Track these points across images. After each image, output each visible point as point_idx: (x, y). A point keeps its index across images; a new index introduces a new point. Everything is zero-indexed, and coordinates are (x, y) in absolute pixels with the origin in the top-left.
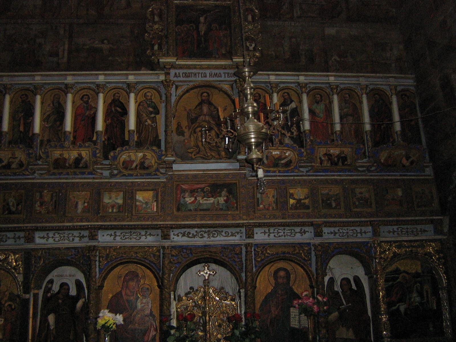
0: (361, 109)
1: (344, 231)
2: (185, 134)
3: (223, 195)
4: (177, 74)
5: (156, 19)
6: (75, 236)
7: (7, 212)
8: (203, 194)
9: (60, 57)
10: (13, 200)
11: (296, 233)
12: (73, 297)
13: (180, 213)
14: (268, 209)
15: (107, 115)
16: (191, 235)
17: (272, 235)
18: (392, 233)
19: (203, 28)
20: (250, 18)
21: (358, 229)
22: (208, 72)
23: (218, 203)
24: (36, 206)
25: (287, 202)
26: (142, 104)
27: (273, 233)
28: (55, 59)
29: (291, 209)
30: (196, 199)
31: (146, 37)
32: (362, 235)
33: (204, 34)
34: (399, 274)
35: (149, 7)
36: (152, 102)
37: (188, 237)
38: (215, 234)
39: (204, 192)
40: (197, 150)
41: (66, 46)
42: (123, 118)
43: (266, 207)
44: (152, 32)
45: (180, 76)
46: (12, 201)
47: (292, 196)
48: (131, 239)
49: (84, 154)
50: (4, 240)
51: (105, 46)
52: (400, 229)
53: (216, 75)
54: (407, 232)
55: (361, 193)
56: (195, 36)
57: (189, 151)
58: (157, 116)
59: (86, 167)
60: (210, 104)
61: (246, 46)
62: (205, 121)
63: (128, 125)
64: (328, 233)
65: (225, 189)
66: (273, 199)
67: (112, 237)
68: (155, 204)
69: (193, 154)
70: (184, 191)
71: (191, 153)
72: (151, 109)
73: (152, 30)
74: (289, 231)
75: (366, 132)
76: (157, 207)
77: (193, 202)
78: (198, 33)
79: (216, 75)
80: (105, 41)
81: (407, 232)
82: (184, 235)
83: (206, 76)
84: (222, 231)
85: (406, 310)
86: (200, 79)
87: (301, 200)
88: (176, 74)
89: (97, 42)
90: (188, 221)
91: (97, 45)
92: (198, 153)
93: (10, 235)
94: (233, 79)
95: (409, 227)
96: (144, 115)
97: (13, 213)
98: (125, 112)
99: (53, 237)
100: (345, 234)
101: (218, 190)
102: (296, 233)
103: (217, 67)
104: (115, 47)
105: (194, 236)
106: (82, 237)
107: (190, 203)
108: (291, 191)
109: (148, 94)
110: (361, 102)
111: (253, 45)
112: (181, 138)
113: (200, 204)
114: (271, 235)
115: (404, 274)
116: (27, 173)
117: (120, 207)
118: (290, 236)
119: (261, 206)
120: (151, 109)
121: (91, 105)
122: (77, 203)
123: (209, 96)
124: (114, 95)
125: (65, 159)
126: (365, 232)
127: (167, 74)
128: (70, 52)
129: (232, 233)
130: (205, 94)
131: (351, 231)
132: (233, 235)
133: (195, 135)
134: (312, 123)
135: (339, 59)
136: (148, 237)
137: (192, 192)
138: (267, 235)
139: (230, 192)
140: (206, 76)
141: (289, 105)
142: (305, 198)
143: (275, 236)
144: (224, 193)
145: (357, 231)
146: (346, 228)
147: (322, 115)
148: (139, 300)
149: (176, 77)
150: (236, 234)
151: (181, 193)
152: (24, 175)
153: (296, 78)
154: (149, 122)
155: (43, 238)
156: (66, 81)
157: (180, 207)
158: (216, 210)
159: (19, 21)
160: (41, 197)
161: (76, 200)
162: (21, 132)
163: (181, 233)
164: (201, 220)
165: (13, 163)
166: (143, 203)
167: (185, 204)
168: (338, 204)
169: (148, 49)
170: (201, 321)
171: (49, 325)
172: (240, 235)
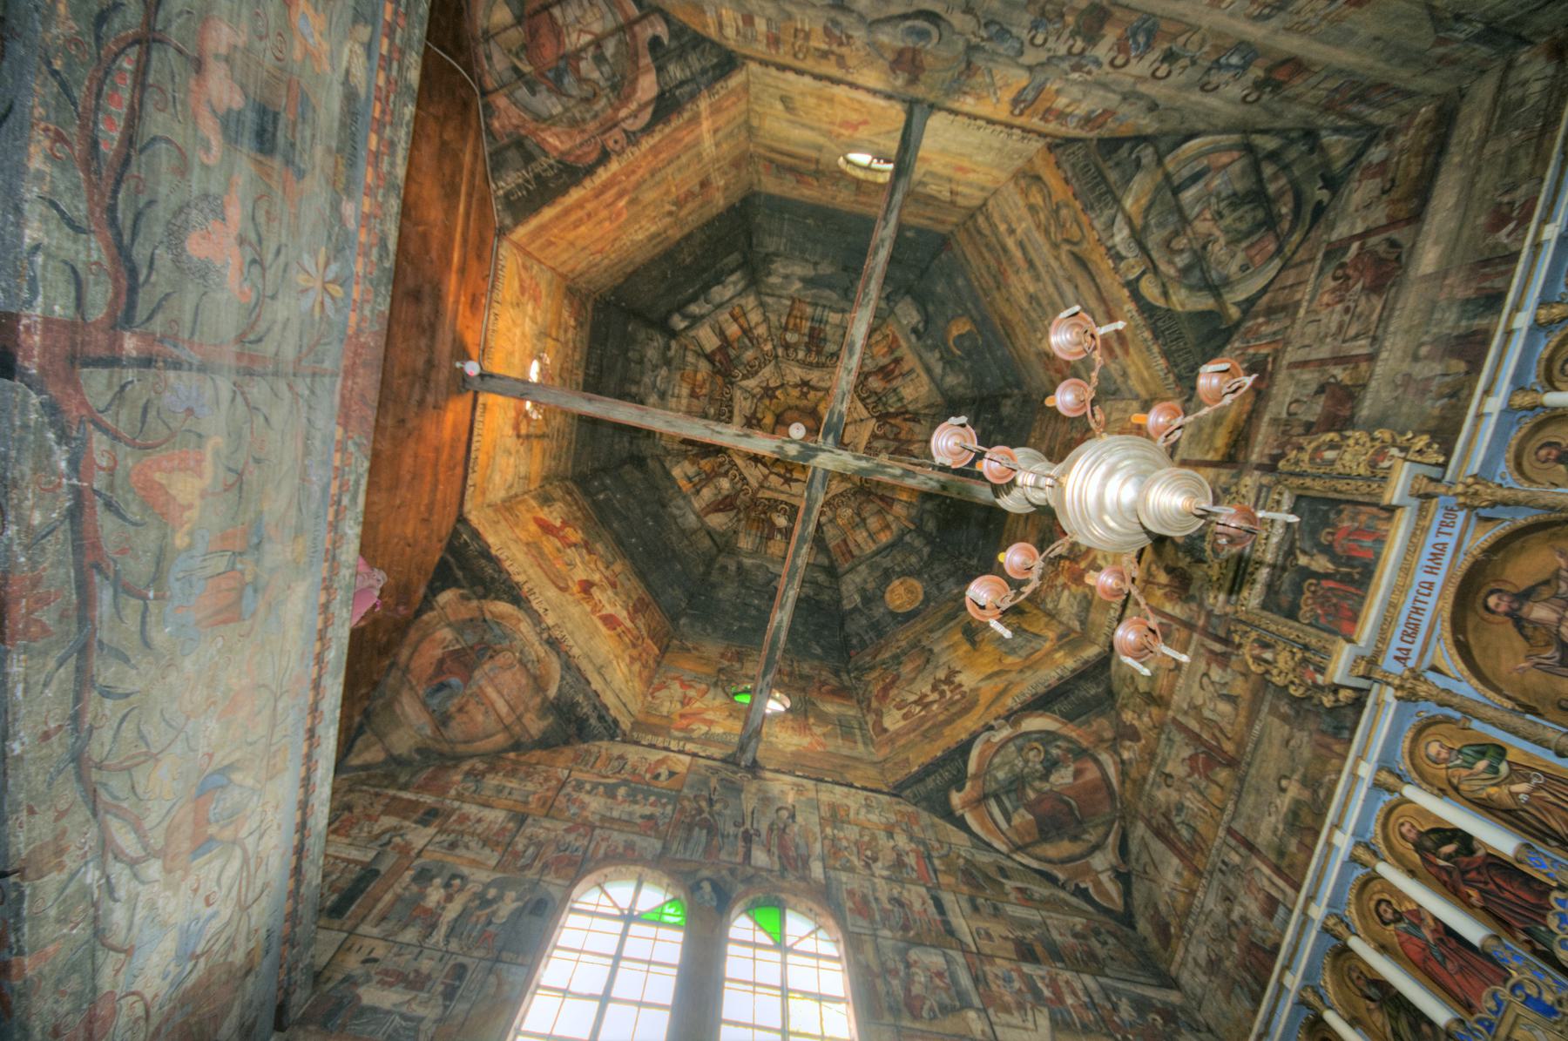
4: (1399, 654)
5: (1268, 655)
15: (1451, 889)
19: (1321, 564)
20: (1329, 455)
22: (1421, 576)
26: (1455, 781)
31: (1297, 694)
33: (1334, 563)
36: (1460, 752)
41: (1266, 870)
42: (1481, 853)
45: (1408, 650)
51: (1294, 790)
56: (1331, 584)
58: (1509, 757)
60: (1527, 595)
78: (1327, 576)
79: (1435, 557)
80: (1284, 783)
83: (1432, 584)
86: (1432, 600)
88: (1397, 658)
89: (1278, 802)
91: (1284, 803)
96: (1493, 790)
98: (1465, 841)
103: (1412, 548)
104: (1302, 770)
109: (1434, 749)
120: (1481, 765)
121: (1409, 912)
123: (1500, 591)
124: (1403, 836)
128: (1277, 870)
135: (1511, 226)
154: (1521, 788)
159: (1190, 922)
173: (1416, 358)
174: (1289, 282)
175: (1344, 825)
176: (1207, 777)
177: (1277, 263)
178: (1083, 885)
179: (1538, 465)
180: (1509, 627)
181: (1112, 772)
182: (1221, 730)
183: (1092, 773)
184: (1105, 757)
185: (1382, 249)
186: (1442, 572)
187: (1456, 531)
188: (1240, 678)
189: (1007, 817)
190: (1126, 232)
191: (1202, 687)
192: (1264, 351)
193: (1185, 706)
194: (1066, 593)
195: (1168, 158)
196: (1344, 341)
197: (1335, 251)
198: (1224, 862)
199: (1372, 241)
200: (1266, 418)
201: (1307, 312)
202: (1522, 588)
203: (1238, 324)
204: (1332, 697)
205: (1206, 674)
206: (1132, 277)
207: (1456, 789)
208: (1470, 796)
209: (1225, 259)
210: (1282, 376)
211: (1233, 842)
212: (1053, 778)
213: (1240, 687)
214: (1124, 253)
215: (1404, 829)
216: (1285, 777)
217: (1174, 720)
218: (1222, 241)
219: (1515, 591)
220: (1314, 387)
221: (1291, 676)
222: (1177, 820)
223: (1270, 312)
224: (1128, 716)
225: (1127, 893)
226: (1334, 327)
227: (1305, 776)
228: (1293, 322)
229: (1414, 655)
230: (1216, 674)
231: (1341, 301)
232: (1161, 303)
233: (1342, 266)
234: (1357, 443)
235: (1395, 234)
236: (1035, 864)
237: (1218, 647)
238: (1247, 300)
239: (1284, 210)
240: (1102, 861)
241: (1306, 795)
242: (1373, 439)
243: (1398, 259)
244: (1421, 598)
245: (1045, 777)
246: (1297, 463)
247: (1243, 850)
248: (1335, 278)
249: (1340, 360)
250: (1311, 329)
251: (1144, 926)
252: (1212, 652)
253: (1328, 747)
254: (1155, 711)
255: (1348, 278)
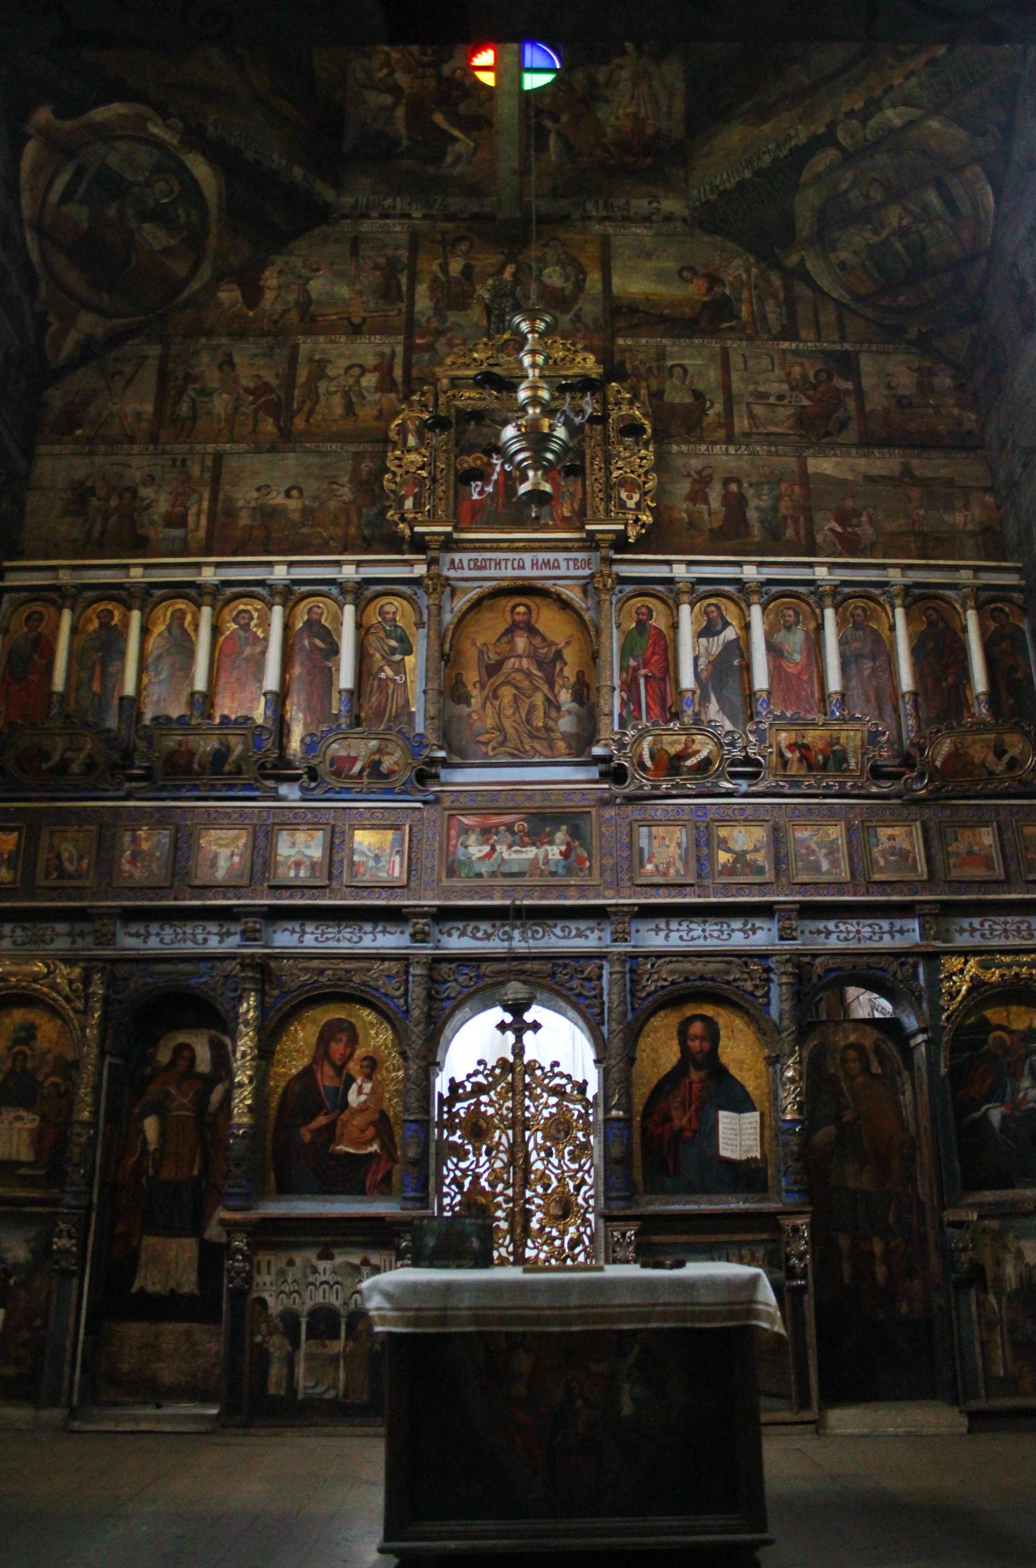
0: (893, 644)
1: (851, 928)
2: (473, 700)
3: (557, 841)
4: (457, 562)
5: (412, 441)
6: (209, 933)
7: (55, 875)
8: (509, 838)
9: (191, 524)
10: (70, 846)
11: (733, 931)
12: (201, 1077)
13: (455, 882)
14: (665, 874)
16: (480, 935)
17: (674, 936)
18: (966, 935)
21: (885, 924)
22: (527, 557)
23: (547, 861)
24: (123, 861)
25: (712, 858)
27: (678, 930)
28: (178, 532)
29: (721, 873)
30: (493, 849)
32: (893, 937)
34: (988, 1033)
35: (396, 414)
36: (396, 626)
37: (474, 937)
38: (537, 932)
39: (513, 833)
40: (501, 738)
41: (205, 505)
42: (329, 664)
43: (661, 867)
44: (399, 471)
45: (462, 568)
46: (68, 850)
47: (723, 844)
48: (339, 940)
49: (233, 740)
50: (48, 938)
52: (987, 924)
53: (546, 564)
54: (1005, 931)
55: (891, 838)
57: (481, 739)
58: (407, 658)
59: (239, 771)
60: (532, 631)
61: (620, 499)
62: (520, 670)
63: (338, 679)
64: (811, 932)
65: (564, 827)
66: (678, 851)
67: (296, 936)
68: (397, 859)
69: (490, 747)
70: (466, 830)
71: (486, 744)
72: (393, 643)
73: (400, 466)
74: (715, 927)
75: (903, 696)
76: (402, 867)
77: (488, 856)
79: (546, 564)
80: (295, 493)
81: (1005, 931)
82: (463, 934)
83: (523, 568)
84: (555, 926)
85: (1004, 1118)
86: (510, 573)
87: (745, 853)
89: (274, 494)
90: (472, 899)
92: (502, 744)
93: (61, 927)
94: (587, 572)
95: (1009, 919)
96: (378, 656)
97: (70, 877)
98: (334, 650)
99: (158, 934)
100: (851, 935)
101: (548, 829)
102: (733, 931)
105: (488, 937)
106: (223, 936)
107: (480, 858)
108: (723, 832)
109: (389, 608)
110: (892, 628)
111: (636, 497)
112: (464, 709)
113: (503, 859)
114: (671, 934)
115: (998, 1033)
116: (105, 786)
117: (313, 866)
118: (718, 938)
119: (649, 867)
120: (393, 643)
122: (216, 856)
124: (310, 610)
125: (191, 754)
126: (902, 931)
127: (432, 562)
128: (212, 516)
129: (577, 929)
130: (521, 609)
131: (868, 929)
132: (580, 935)
133: (497, 703)
134: (776, 672)
135: (839, 529)
136: (380, 936)
137: (486, 832)
138: (662, 934)
139: (575, 833)
140: (523, 568)
141: (719, 633)
142: (756, 850)
143: (681, 938)
144: (560, 836)
145: (881, 928)
146: (854, 922)
147: (797, 657)
148: (354, 1087)
149: (454, 568)
150: (588, 933)
151: (459, 836)
152: (96, 789)
153: (737, 569)
154: (389, 671)
155: (137, 935)
156: (199, 579)
157: (456, 865)
158: (541, 875)
160: (135, 840)
161: (214, 848)
162: (95, 694)
163: (458, 929)
164: (503, 898)
165: (72, 761)
166: (367, 856)
167: (469, 862)
168: (835, 863)
169: (390, 507)
170: (504, 1140)
171: (145, 1140)
172: (597, 934)
173: (727, 482)
174: (822, 319)
175: (293, 570)
176: (256, 411)
177: (846, 299)
178: (51, 318)
179: (634, 609)
180: (502, 627)
181: (195, 286)
182: (311, 412)
183: (180, 268)
184: (206, 272)
185: (840, 414)
186: (536, 573)
187: (573, 573)
188: (375, 412)
189: (67, 196)
190: (897, 122)
191: (348, 368)
192: (744, 313)
193: (317, 357)
194: (388, 100)
195: (978, 169)
196: (748, 405)
197: (847, 365)
198: (184, 461)
199: (851, 404)
200: (666, 341)
201: (784, 351)
202: (537, 626)
203: (778, 266)
204: (396, 518)
205: (364, 370)
206: (841, 135)
207: (367, 633)
208: (366, 642)
209: (852, 244)
210: (715, 345)
211: (209, 462)
212: (147, 226)
213: (366, 413)
214: (871, 123)
215: (316, 609)
216: (300, 491)
217: (296, 347)
218: (875, 239)
219: (533, 621)
220: (700, 386)
221: (399, 471)
222: (193, 394)
223: (790, 302)
224: (271, 279)
225: (75, 364)
226: (762, 388)
227: (312, 510)
228: (776, 338)
229: (460, 574)
230: (369, 381)
231: (792, 388)
232: (806, 175)
233: (830, 378)
234: (642, 459)
235: (853, 425)
236: (35, 257)
237: (398, 373)
238: (807, 272)
239: (902, 299)
240: (88, 324)
241: (296, 517)
242: (646, 473)
243: (828, 434)
244: (509, 564)
245: (144, 217)
246: (617, 403)
247: (207, 475)
248: (817, 375)
249: (729, 401)
250: (765, 362)
251: (56, 397)
252: (391, 368)
253: (348, 523)
254: (294, 316)
255: (815, 387)
